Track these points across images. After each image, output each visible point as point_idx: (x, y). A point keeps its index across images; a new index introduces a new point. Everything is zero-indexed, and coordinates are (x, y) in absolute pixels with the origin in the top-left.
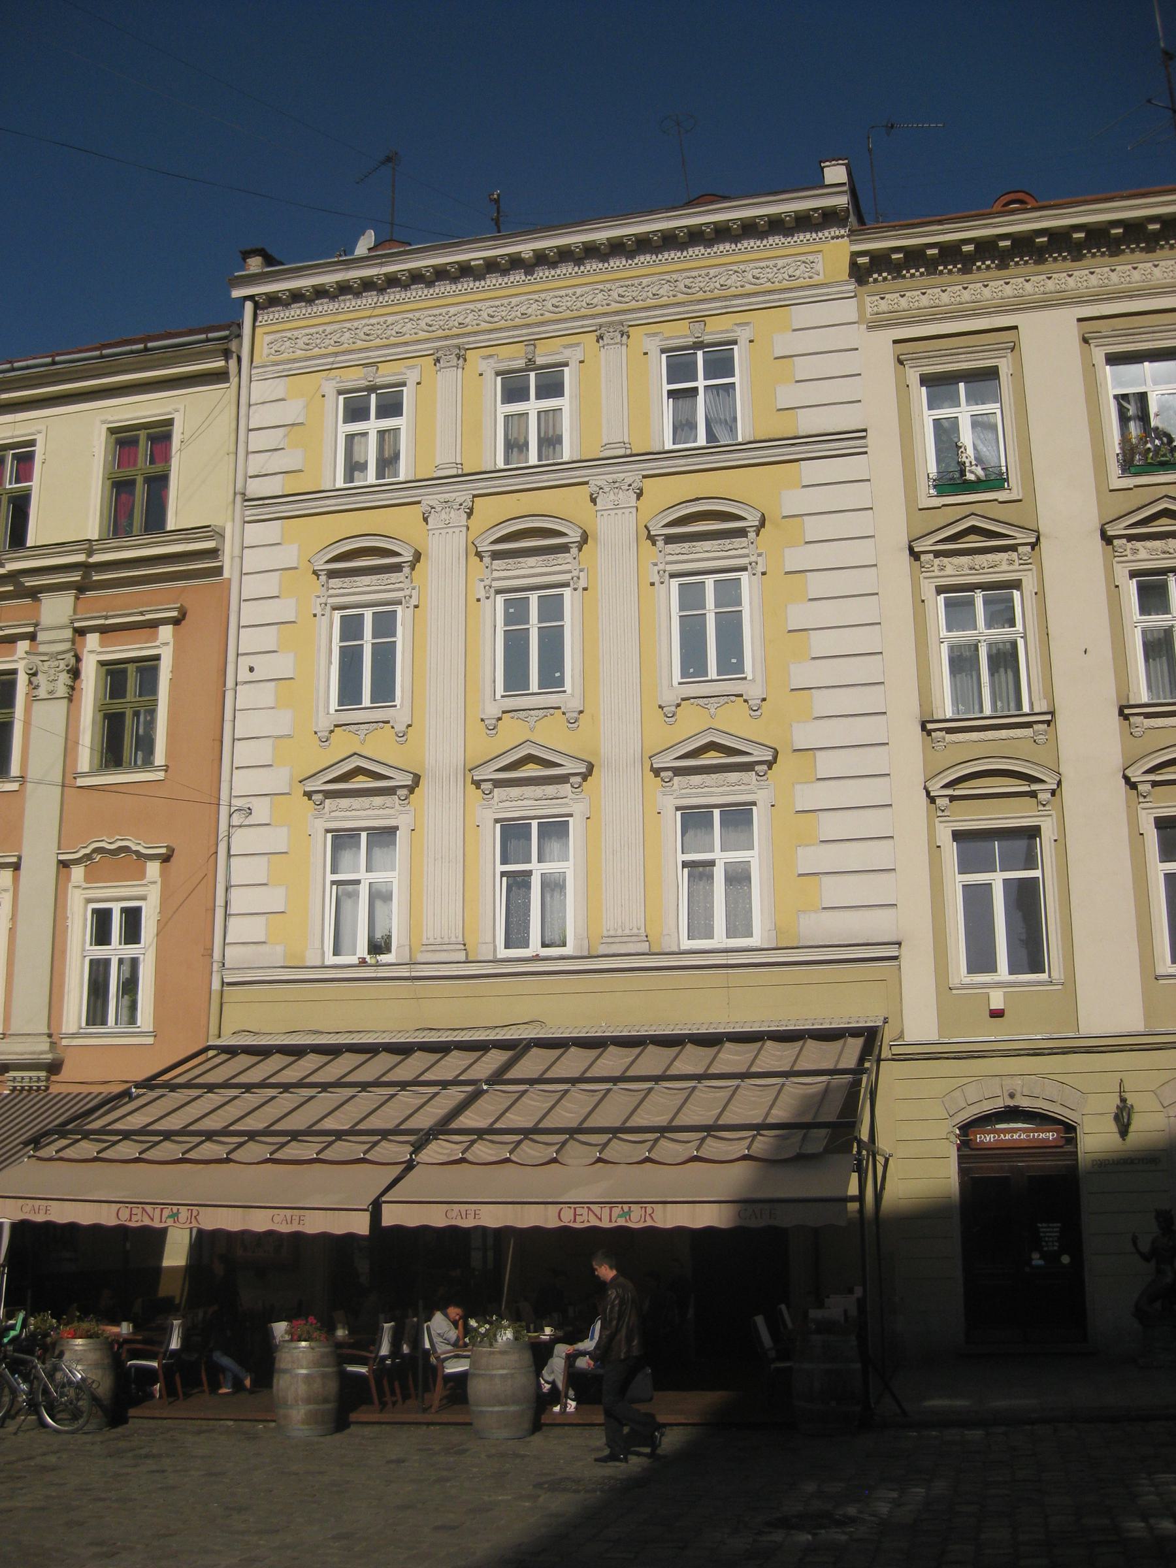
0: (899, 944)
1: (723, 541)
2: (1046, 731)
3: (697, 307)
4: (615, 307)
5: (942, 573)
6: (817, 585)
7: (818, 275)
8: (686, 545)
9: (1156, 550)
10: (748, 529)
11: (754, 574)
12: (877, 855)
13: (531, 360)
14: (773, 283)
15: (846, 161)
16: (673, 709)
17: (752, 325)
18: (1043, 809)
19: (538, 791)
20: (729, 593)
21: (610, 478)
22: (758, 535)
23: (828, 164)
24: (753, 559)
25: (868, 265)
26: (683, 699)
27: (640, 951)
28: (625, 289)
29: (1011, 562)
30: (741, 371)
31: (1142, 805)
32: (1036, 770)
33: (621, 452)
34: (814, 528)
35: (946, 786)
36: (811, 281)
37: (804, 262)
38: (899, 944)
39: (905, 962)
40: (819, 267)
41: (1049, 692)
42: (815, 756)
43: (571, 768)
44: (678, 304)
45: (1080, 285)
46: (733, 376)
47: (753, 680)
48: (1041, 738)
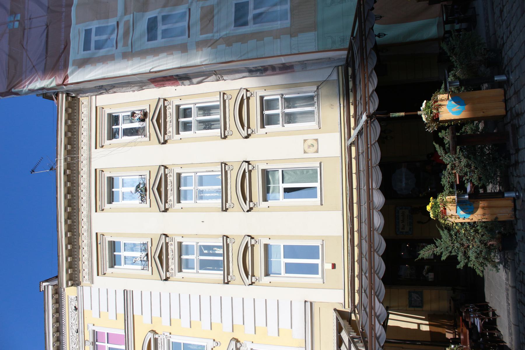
1: (159, 347)
5: (174, 269)
9: (170, 193)
10: (154, 337)
14: (76, 314)
15: (41, 283)
22: (157, 334)
23: (41, 289)
29: (172, 244)
35: (248, 278)
37: (71, 302)
38: (305, 302)
41: (216, 237)
45: (86, 210)
48: (233, 241)
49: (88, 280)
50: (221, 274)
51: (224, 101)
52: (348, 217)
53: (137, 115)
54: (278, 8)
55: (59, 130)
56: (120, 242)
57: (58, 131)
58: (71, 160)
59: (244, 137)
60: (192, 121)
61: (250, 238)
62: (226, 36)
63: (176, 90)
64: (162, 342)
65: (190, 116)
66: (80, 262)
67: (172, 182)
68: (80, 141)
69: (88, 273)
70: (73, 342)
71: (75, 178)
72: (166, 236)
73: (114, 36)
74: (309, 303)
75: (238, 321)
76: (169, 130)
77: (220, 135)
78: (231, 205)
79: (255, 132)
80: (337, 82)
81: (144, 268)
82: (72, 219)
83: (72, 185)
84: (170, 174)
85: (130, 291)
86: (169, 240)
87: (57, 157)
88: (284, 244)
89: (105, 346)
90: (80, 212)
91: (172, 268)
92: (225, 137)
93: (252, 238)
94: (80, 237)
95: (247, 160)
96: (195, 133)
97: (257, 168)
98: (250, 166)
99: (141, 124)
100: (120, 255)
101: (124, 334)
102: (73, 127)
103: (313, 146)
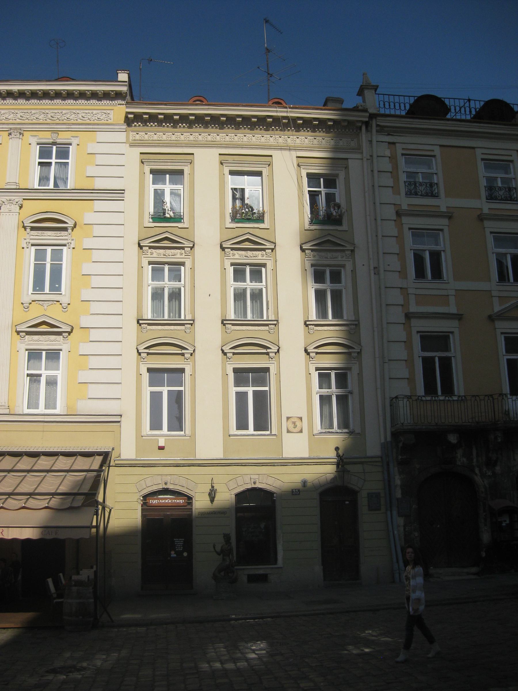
0: (121, 416)
2: (190, 328)
4: (18, 121)
5: (152, 256)
6: (96, 255)
7: (111, 120)
8: (40, 232)
10: (68, 228)
11: (69, 248)
12: (114, 376)
14: (90, 120)
15: (128, 72)
16: (28, 305)
17: (79, 137)
18: (187, 361)
20: (57, 255)
21: (8, 198)
22: (72, 231)
23: (120, 72)
24: (69, 241)
25: (133, 119)
26: (33, 301)
27: (5, 413)
28: (24, 114)
29: (181, 254)
30: (72, 158)
31: (228, 362)
33: (14, 187)
34: (97, 230)
36: (107, 122)
37: (105, 113)
38: (121, 416)
39: (123, 424)
40: (111, 116)
41: (193, 311)
42: (90, 331)
44: (47, 124)
45: (221, 139)
46: (68, 159)
47: (65, 295)
48: (188, 331)
49: (134, 138)
59: (307, 348)
63: (363, 265)
65: (332, 282)
67: (256, 258)
74: (119, 420)
92: (307, 325)
93: (191, 354)
97: (270, 362)
98: (274, 354)
103: (294, 428)
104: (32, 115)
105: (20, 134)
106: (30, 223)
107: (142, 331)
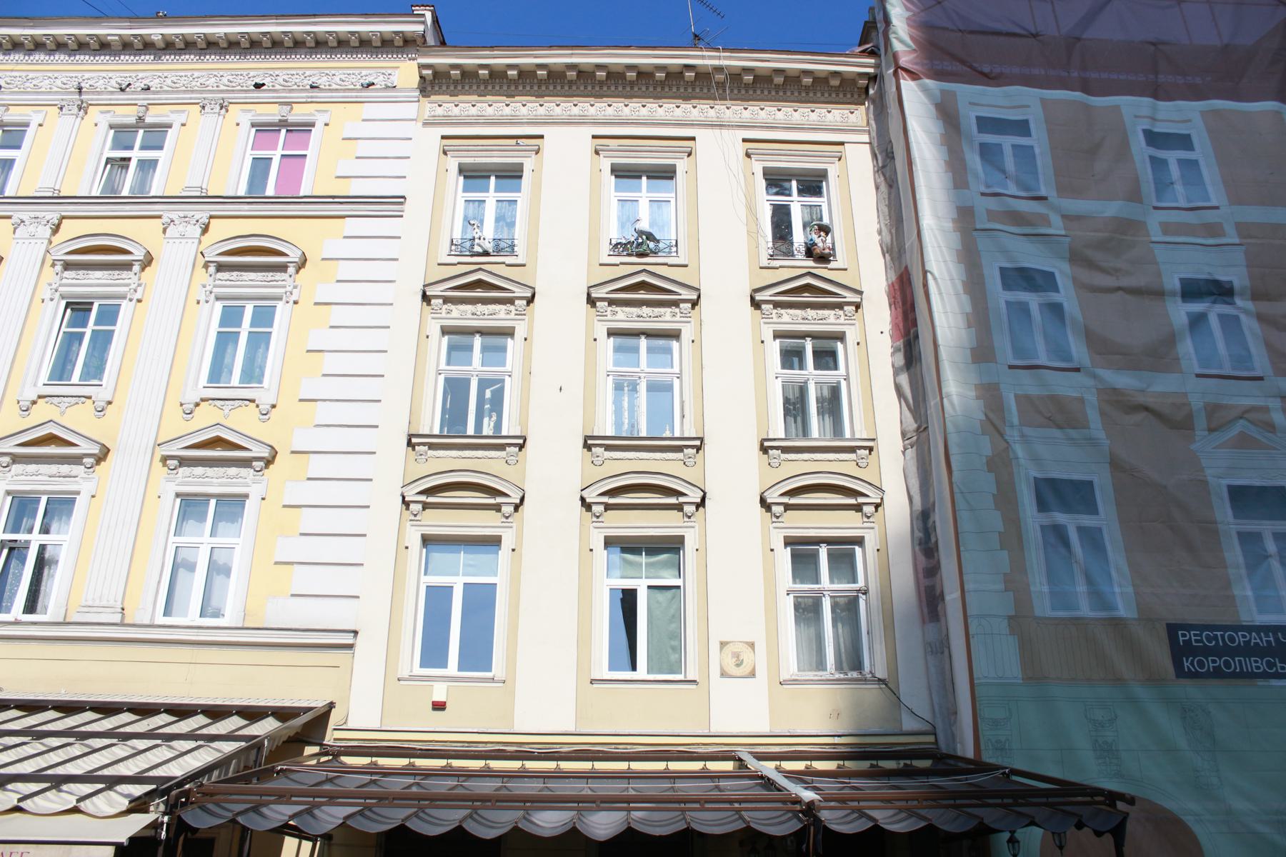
0: (356, 633)
3: (288, 95)
5: (449, 316)
8: (235, 273)
10: (289, 264)
13: (140, 119)
14: (355, 86)
15: (432, 8)
19: (53, 469)
22: (297, 272)
23: (417, 8)
29: (509, 312)
32: (502, 485)
33: (198, 194)
35: (421, 493)
37: (383, 74)
38: (356, 633)
41: (524, 421)
43: (85, 449)
45: (599, 113)
50: (431, 428)
51: (852, 450)
52: (558, 746)
53: (822, 240)
54: (1081, 588)
55: (790, 57)
56: (519, 190)
57: (788, 55)
58: (718, 83)
59: (765, 494)
60: (806, 370)
61: (518, 501)
62: (1011, 456)
63: (882, 333)
64: (277, 281)
66: (475, 98)
68: (762, 104)
69: (450, 113)
70: (290, 76)
71: (674, 90)
72: (530, 300)
73: (1012, 189)
74: (350, 642)
75: (318, 466)
76: (785, 315)
77: (770, 437)
78: (599, 458)
79: (776, 522)
80: (896, 731)
81: (456, 245)
82: (578, 82)
83: (659, 83)
84: (678, 314)
85: (402, 211)
86: (520, 307)
87: (725, 50)
88: (498, 586)
89: (276, 149)
90: (593, 99)
91: (451, 311)
92: (764, 450)
93: (517, 508)
94: (534, 98)
95: (707, 501)
96: (777, 378)
97: (685, 524)
98: (693, 508)
99: (801, 247)
100: (487, 191)
101: (302, 194)
102: (796, 87)
103: (738, 665)
104: (249, 78)
105: (221, 108)
106: (217, 255)
107: (416, 460)
